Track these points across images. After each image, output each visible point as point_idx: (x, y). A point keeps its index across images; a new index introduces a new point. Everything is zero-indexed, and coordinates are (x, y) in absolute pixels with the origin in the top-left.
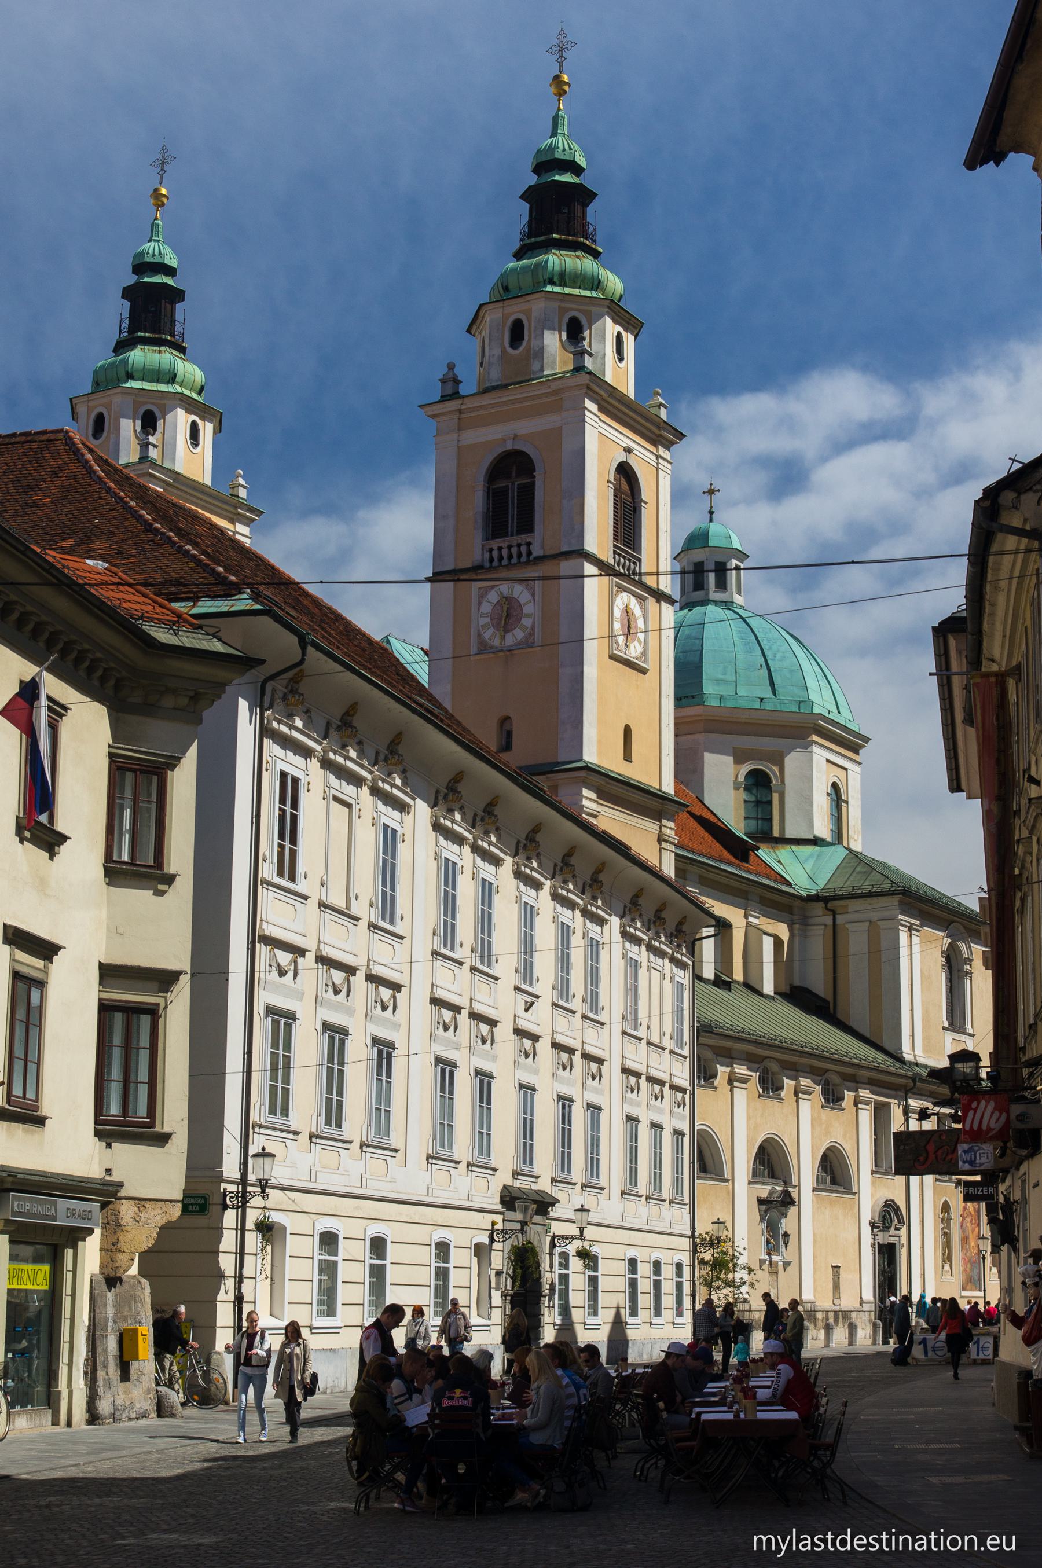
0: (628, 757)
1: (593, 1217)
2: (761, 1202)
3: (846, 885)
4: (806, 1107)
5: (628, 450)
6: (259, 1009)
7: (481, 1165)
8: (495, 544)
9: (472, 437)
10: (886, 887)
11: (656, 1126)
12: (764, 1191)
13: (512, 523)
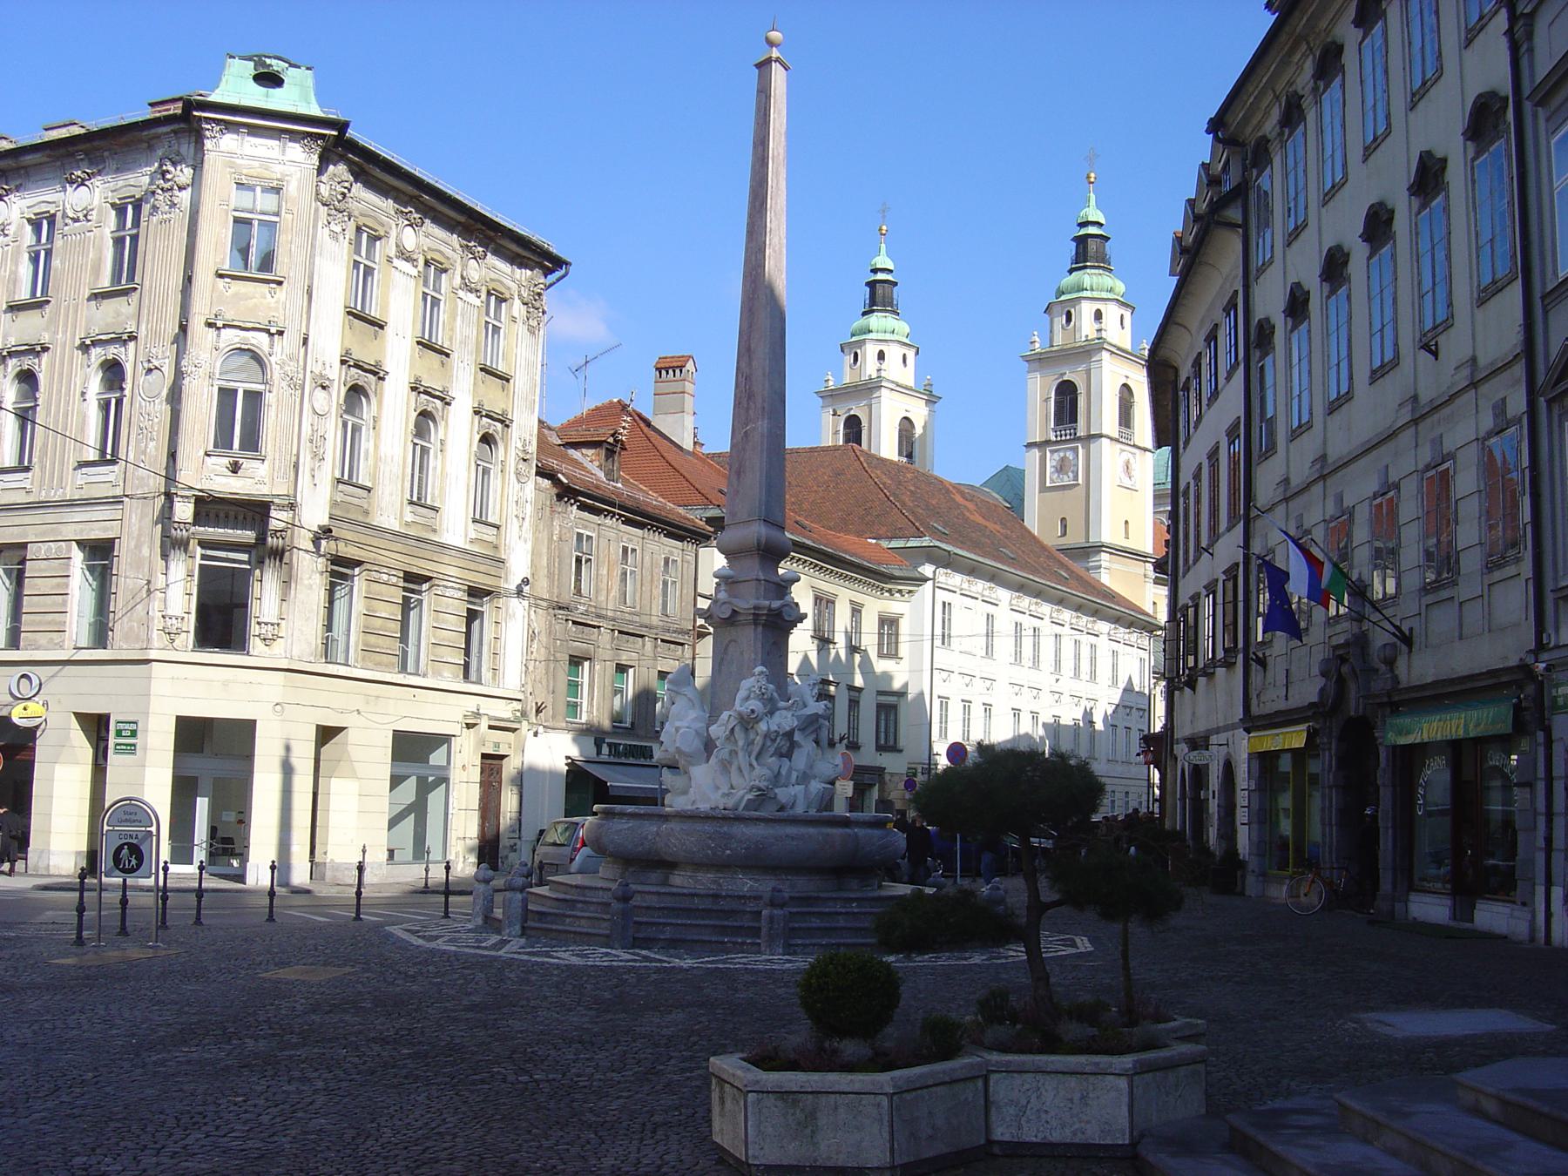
6: (935, 697)
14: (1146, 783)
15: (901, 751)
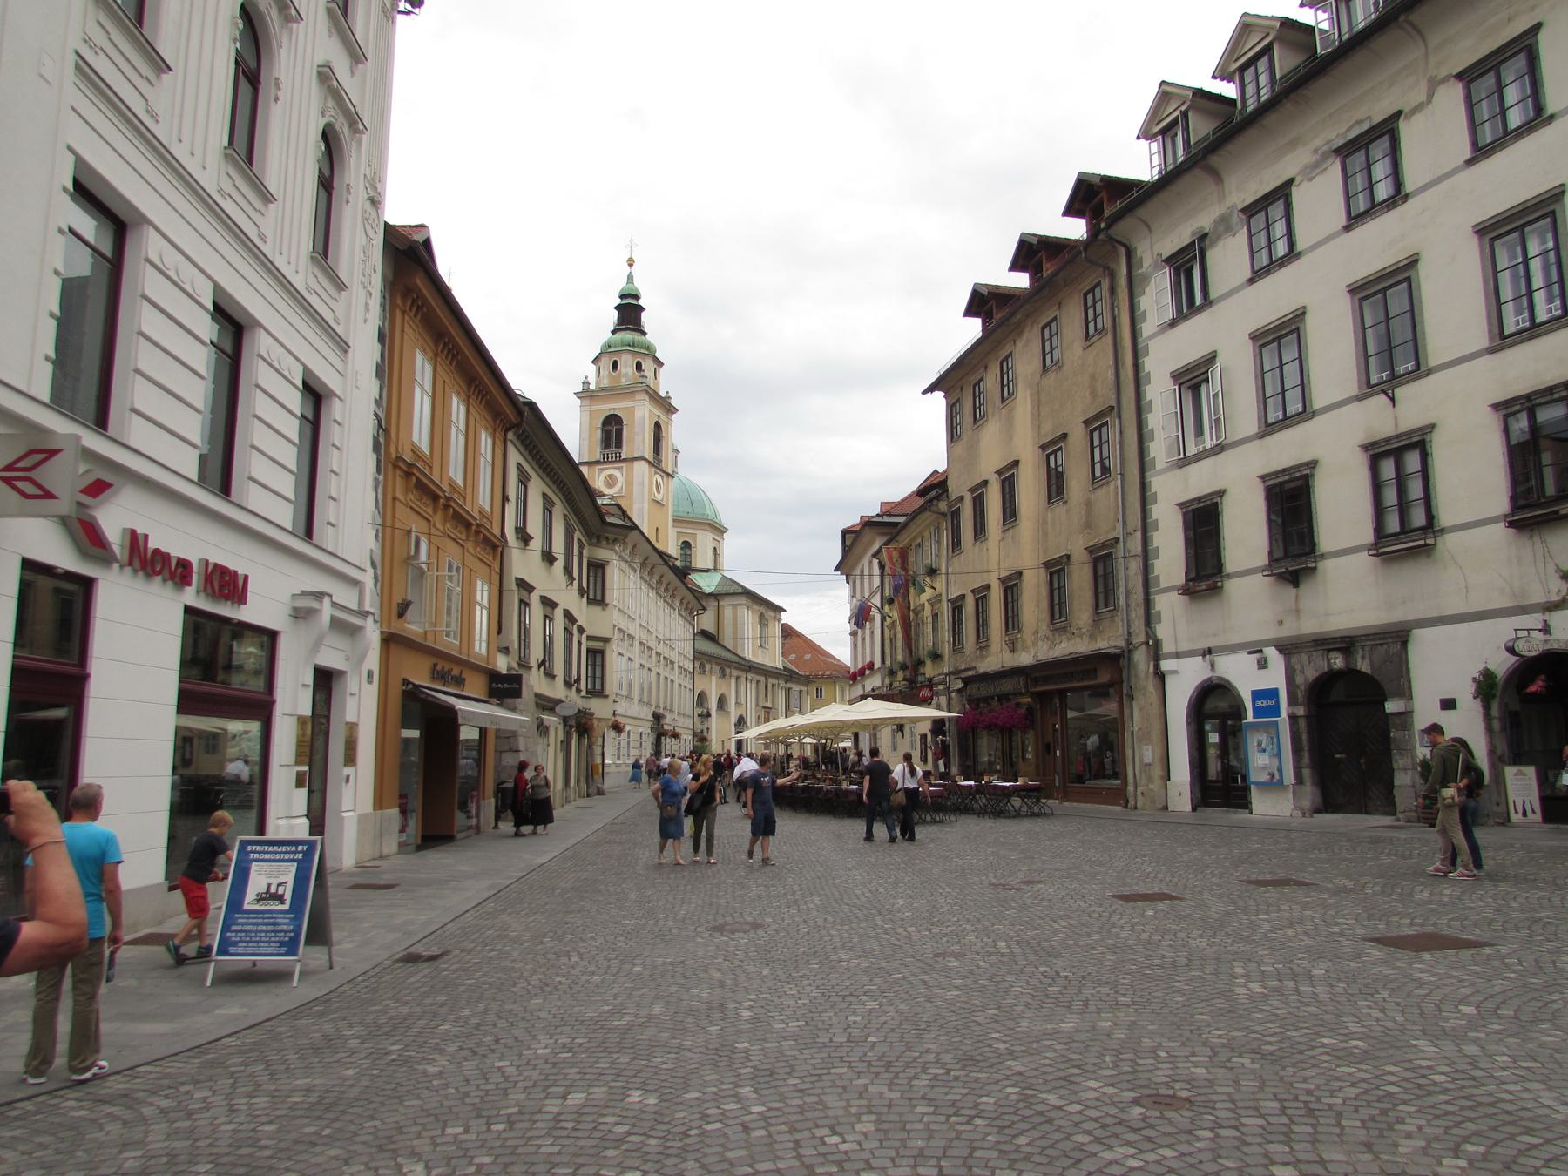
3: (723, 590)
4: (714, 678)
5: (659, 416)
7: (649, 704)
8: (606, 452)
9: (595, 408)
10: (740, 590)
12: (698, 711)
13: (613, 444)
14: (691, 732)
15: (607, 697)
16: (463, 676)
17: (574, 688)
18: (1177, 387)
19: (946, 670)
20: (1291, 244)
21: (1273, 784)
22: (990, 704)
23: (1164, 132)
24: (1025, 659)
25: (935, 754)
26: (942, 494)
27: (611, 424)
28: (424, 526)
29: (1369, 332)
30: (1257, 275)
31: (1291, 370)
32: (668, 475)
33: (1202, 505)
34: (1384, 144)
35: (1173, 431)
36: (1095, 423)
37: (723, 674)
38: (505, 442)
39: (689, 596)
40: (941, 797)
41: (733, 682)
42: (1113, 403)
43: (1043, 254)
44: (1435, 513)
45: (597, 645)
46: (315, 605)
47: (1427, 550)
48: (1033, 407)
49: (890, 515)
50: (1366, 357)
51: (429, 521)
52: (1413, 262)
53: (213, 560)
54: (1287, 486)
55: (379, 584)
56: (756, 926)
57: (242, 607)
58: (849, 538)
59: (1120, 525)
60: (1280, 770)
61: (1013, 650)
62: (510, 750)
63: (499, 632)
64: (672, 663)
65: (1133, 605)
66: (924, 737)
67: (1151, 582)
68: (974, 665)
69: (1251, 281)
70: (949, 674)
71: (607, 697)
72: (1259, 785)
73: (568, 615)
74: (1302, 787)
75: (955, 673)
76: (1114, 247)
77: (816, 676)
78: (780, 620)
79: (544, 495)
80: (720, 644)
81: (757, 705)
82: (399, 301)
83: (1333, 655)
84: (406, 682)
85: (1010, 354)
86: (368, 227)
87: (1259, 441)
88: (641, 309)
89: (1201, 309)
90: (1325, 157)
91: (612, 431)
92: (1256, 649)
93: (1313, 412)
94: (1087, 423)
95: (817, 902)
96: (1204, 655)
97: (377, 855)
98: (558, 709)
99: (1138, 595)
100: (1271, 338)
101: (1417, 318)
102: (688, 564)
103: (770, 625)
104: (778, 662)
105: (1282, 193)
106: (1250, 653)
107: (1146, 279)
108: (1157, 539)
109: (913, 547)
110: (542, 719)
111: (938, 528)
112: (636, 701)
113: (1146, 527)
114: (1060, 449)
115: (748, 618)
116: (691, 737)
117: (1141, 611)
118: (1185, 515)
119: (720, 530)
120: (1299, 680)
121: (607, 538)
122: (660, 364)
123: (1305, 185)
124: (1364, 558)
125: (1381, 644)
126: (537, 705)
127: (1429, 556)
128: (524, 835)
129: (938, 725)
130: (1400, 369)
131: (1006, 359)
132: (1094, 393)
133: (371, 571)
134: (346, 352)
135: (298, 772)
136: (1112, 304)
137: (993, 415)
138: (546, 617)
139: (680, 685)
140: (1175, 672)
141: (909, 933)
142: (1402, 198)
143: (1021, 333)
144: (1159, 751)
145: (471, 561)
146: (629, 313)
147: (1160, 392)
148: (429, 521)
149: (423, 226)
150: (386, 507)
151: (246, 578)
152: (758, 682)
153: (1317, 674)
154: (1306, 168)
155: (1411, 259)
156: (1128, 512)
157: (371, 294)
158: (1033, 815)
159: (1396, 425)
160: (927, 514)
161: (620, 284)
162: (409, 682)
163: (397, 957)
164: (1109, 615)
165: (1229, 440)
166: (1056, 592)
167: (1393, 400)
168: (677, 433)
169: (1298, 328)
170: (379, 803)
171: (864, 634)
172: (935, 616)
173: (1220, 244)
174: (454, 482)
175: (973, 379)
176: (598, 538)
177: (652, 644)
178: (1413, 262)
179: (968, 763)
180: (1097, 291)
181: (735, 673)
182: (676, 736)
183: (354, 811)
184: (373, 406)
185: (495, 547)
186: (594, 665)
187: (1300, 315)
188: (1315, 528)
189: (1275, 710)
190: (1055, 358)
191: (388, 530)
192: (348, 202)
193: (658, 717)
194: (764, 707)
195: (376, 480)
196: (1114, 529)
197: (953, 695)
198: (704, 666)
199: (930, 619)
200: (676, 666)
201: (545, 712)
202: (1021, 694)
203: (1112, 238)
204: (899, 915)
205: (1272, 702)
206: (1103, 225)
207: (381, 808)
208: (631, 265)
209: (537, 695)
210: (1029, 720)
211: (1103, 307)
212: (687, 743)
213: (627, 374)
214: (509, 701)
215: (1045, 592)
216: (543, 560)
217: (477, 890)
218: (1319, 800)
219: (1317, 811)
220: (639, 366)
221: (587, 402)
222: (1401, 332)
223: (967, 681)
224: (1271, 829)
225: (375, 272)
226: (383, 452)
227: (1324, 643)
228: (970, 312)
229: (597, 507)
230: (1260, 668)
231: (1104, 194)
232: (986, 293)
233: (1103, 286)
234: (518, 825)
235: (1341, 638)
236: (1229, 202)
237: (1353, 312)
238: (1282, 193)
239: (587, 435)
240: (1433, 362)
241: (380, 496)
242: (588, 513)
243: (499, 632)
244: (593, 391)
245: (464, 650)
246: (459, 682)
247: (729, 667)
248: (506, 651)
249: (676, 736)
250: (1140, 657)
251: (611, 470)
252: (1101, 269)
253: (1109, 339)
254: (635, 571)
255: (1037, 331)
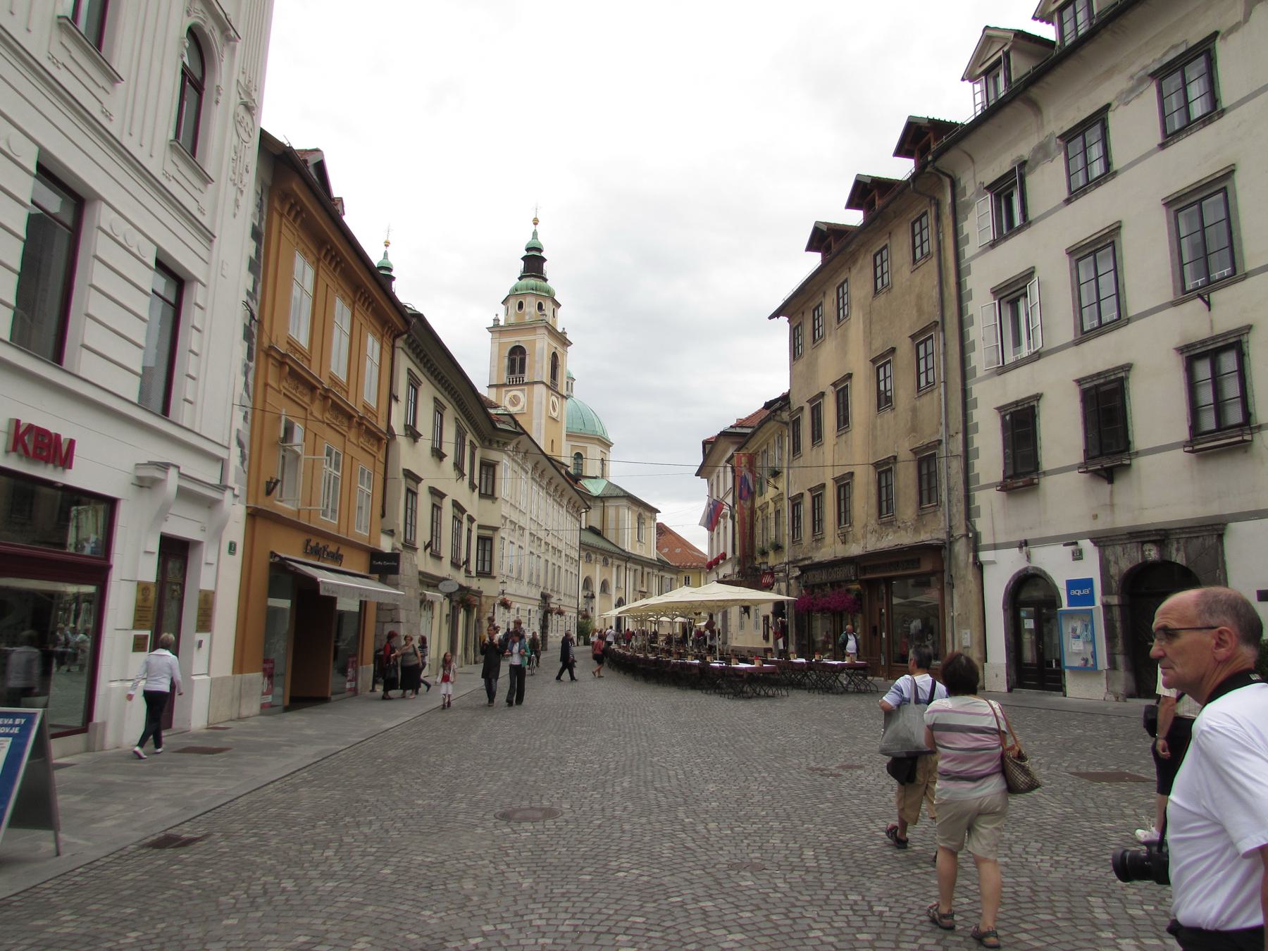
0: (552, 451)
1: (562, 603)
2: (585, 597)
4: (598, 566)
7: (537, 585)
8: (511, 377)
10: (622, 494)
11: (571, 573)
15: (494, 577)
16: (340, 552)
17: (463, 570)
18: (997, 302)
19: (786, 560)
20: (1108, 164)
21: (1088, 669)
22: (823, 590)
23: (986, 73)
24: (855, 550)
25: (775, 633)
26: (785, 405)
27: (515, 354)
28: (301, 413)
29: (1184, 242)
30: (1074, 195)
31: (1107, 283)
32: (563, 396)
33: (1019, 408)
34: (1200, 64)
35: (993, 341)
36: (921, 337)
37: (606, 563)
38: (393, 347)
39: (576, 497)
40: (773, 673)
41: (614, 569)
42: (938, 319)
43: (875, 192)
44: (1252, 410)
45: (488, 533)
46: (158, 474)
47: (1243, 446)
48: (865, 327)
49: (742, 427)
50: (1182, 265)
51: (306, 409)
52: (1229, 173)
53: (26, 420)
54: (1103, 389)
55: (246, 463)
56: (550, 813)
57: (68, 471)
58: (708, 447)
59: (943, 428)
60: (1094, 655)
61: (844, 543)
62: (392, 621)
63: (383, 515)
64: (560, 551)
65: (954, 501)
66: (766, 618)
67: (972, 480)
68: (810, 555)
69: (1068, 201)
70: (788, 563)
71: (494, 577)
72: (1074, 669)
73: (456, 504)
74: (1117, 672)
75: (793, 562)
76: (940, 179)
77: (685, 567)
78: (655, 520)
79: (436, 400)
80: (604, 538)
81: (634, 590)
82: (277, 204)
83: (1147, 547)
84: (273, 554)
85: (846, 281)
86: (241, 131)
87: (1075, 347)
88: (544, 260)
89: (1020, 229)
90: (1141, 81)
91: (517, 359)
92: (1071, 540)
93: (1128, 319)
94: (913, 337)
95: (625, 784)
96: (1020, 547)
97: (235, 716)
98: (441, 586)
99: (959, 492)
100: (1087, 252)
101: (1233, 225)
102: (580, 471)
103: (647, 521)
104: (652, 554)
105: (1099, 118)
106: (1065, 545)
107: (969, 206)
108: (978, 441)
109: (760, 453)
110: (425, 595)
111: (781, 436)
112: (525, 582)
113: (967, 429)
114: (889, 362)
115: (628, 517)
116: (575, 615)
117: (962, 507)
118: (1003, 418)
119: (607, 445)
120: (1113, 570)
121: (498, 442)
122: (558, 305)
123: (1121, 109)
124: (1180, 455)
125: (1198, 537)
126: (421, 582)
127: (1246, 452)
128: (390, 699)
129: (779, 607)
130: (1216, 275)
131: (842, 285)
132: (920, 311)
133: (236, 451)
134: (211, 241)
135: (136, 637)
136: (938, 233)
137: (830, 334)
138: (434, 505)
139: (567, 570)
140: (993, 562)
141: (709, 831)
142: (1218, 114)
143: (855, 262)
144: (977, 635)
145: (352, 450)
146: (534, 263)
147: (982, 308)
148: (306, 409)
149: (317, 150)
150: (257, 394)
151: (72, 443)
152: (635, 570)
153: (1130, 566)
154: (1122, 93)
155: (1227, 171)
156: (950, 417)
157: (242, 192)
158: (860, 692)
159: (1212, 328)
160: (772, 423)
161: (527, 239)
162: (276, 555)
163: (148, 841)
164: (932, 510)
165: (1046, 348)
166: (884, 490)
167: (1208, 304)
168: (573, 363)
169: (1113, 242)
170: (240, 665)
171: (719, 529)
172: (777, 512)
173: (1038, 170)
174: (337, 378)
175: (813, 304)
176: (490, 441)
177: (542, 534)
178: (1229, 173)
179: (805, 642)
180: (924, 220)
181: (617, 562)
182: (561, 613)
183: (208, 674)
184: (245, 298)
185: (379, 440)
186: (484, 550)
187: (1116, 229)
188: (1130, 427)
189: (1089, 599)
190: (886, 281)
191: (258, 413)
192: (217, 102)
193: (545, 597)
194: (640, 592)
195: (246, 366)
196: (937, 432)
197: (792, 581)
198: (590, 556)
199: (773, 515)
200: (563, 554)
201: (430, 588)
202: (852, 582)
203: (937, 170)
204: (704, 804)
205: (1086, 592)
206: (930, 158)
207: (241, 672)
208: (536, 224)
209: (420, 573)
210: (857, 605)
211: (929, 233)
212: (572, 619)
213: (530, 312)
214: (392, 577)
215: (873, 490)
216: (433, 455)
217: (305, 754)
218: (1132, 685)
219: (1131, 696)
220: (540, 307)
221: (497, 335)
222: (1216, 239)
223: (804, 570)
224: (1088, 713)
225: (248, 172)
226: (255, 340)
227: (1139, 536)
228: (811, 247)
229: (488, 415)
230: (1074, 560)
231: (931, 135)
232: (825, 230)
233: (929, 215)
234: (386, 690)
235: (1156, 530)
236: (1047, 133)
237: (1169, 223)
238: (1099, 118)
239: (495, 364)
240: (1248, 268)
241: (251, 382)
242: (479, 418)
243: (383, 515)
244: (502, 326)
245: (343, 530)
246: (337, 558)
247: (611, 557)
248: (391, 533)
249: (561, 613)
250: (961, 548)
251: (515, 392)
252: (928, 199)
253: (934, 261)
254: (527, 473)
255: (870, 258)
